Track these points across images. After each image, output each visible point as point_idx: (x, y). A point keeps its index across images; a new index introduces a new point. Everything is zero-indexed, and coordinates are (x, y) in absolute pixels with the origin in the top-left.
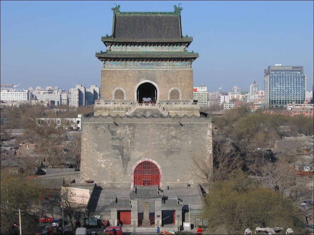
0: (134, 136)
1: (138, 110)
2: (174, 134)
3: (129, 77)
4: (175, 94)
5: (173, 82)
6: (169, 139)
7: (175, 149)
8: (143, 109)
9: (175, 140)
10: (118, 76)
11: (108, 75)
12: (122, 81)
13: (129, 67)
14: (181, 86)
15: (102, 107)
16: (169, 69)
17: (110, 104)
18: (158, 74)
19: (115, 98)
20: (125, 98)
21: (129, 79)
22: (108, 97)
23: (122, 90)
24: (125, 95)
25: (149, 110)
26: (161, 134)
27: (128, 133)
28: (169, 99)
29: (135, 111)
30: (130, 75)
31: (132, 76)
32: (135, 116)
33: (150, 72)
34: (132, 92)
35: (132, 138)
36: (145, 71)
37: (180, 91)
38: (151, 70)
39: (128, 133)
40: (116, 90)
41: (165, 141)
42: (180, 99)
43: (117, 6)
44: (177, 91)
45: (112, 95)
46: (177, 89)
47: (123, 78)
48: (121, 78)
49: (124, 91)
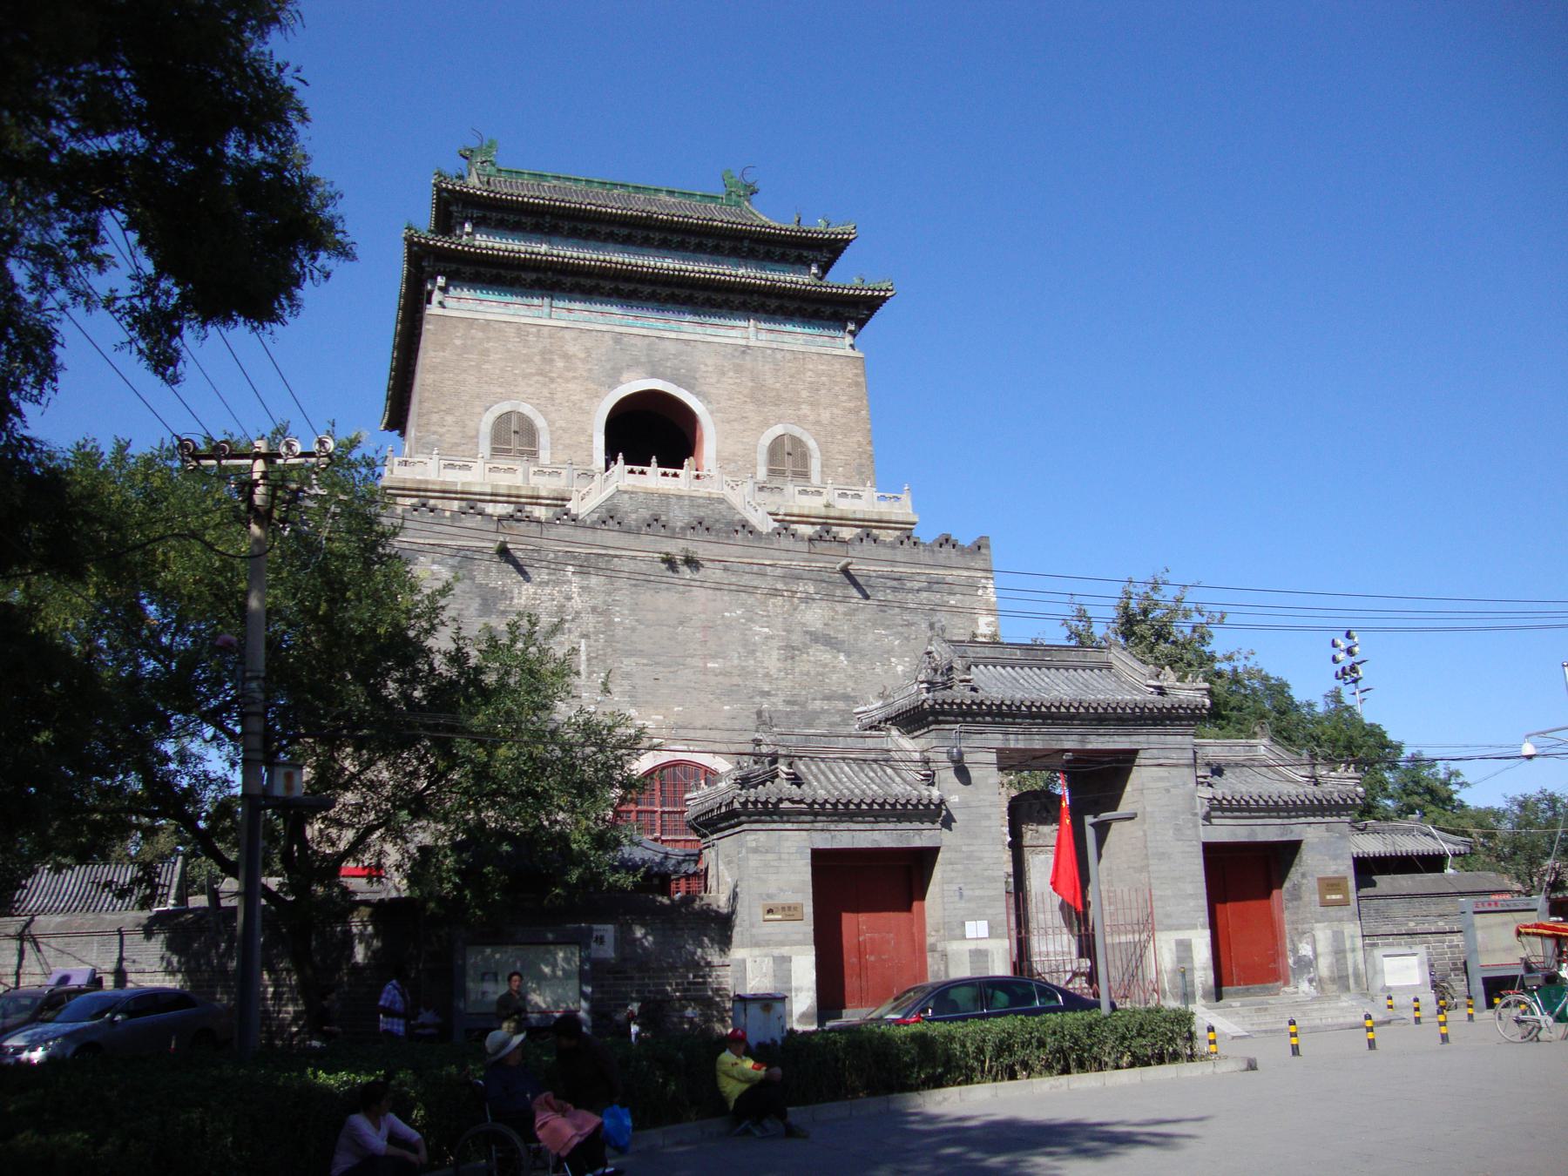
0: (610, 623)
1: (626, 496)
2: (819, 625)
3: (566, 357)
4: (787, 459)
5: (778, 401)
6: (793, 648)
7: (827, 698)
8: (649, 494)
9: (821, 654)
10: (508, 351)
11: (458, 342)
12: (532, 374)
13: (565, 314)
14: (818, 422)
15: (427, 482)
16: (759, 344)
17: (469, 468)
18: (708, 360)
19: (496, 451)
20: (545, 456)
21: (567, 369)
22: (457, 445)
23: (532, 416)
24: (544, 439)
25: (680, 497)
26: (750, 620)
27: (577, 603)
28: (762, 473)
29: (612, 497)
30: (572, 349)
31: (583, 355)
32: (610, 517)
33: (671, 348)
34: (583, 431)
35: (597, 633)
36: (647, 341)
37: (812, 444)
38: (673, 335)
39: (577, 603)
40: (497, 414)
41: (775, 654)
42: (815, 477)
43: (486, 142)
44: (797, 442)
45: (477, 437)
46: (797, 431)
47: (537, 359)
48: (528, 360)
49: (540, 423)
